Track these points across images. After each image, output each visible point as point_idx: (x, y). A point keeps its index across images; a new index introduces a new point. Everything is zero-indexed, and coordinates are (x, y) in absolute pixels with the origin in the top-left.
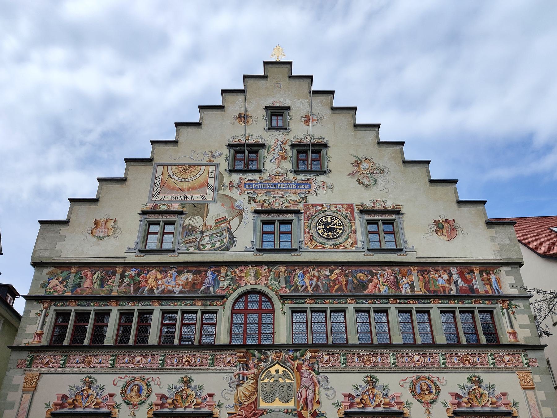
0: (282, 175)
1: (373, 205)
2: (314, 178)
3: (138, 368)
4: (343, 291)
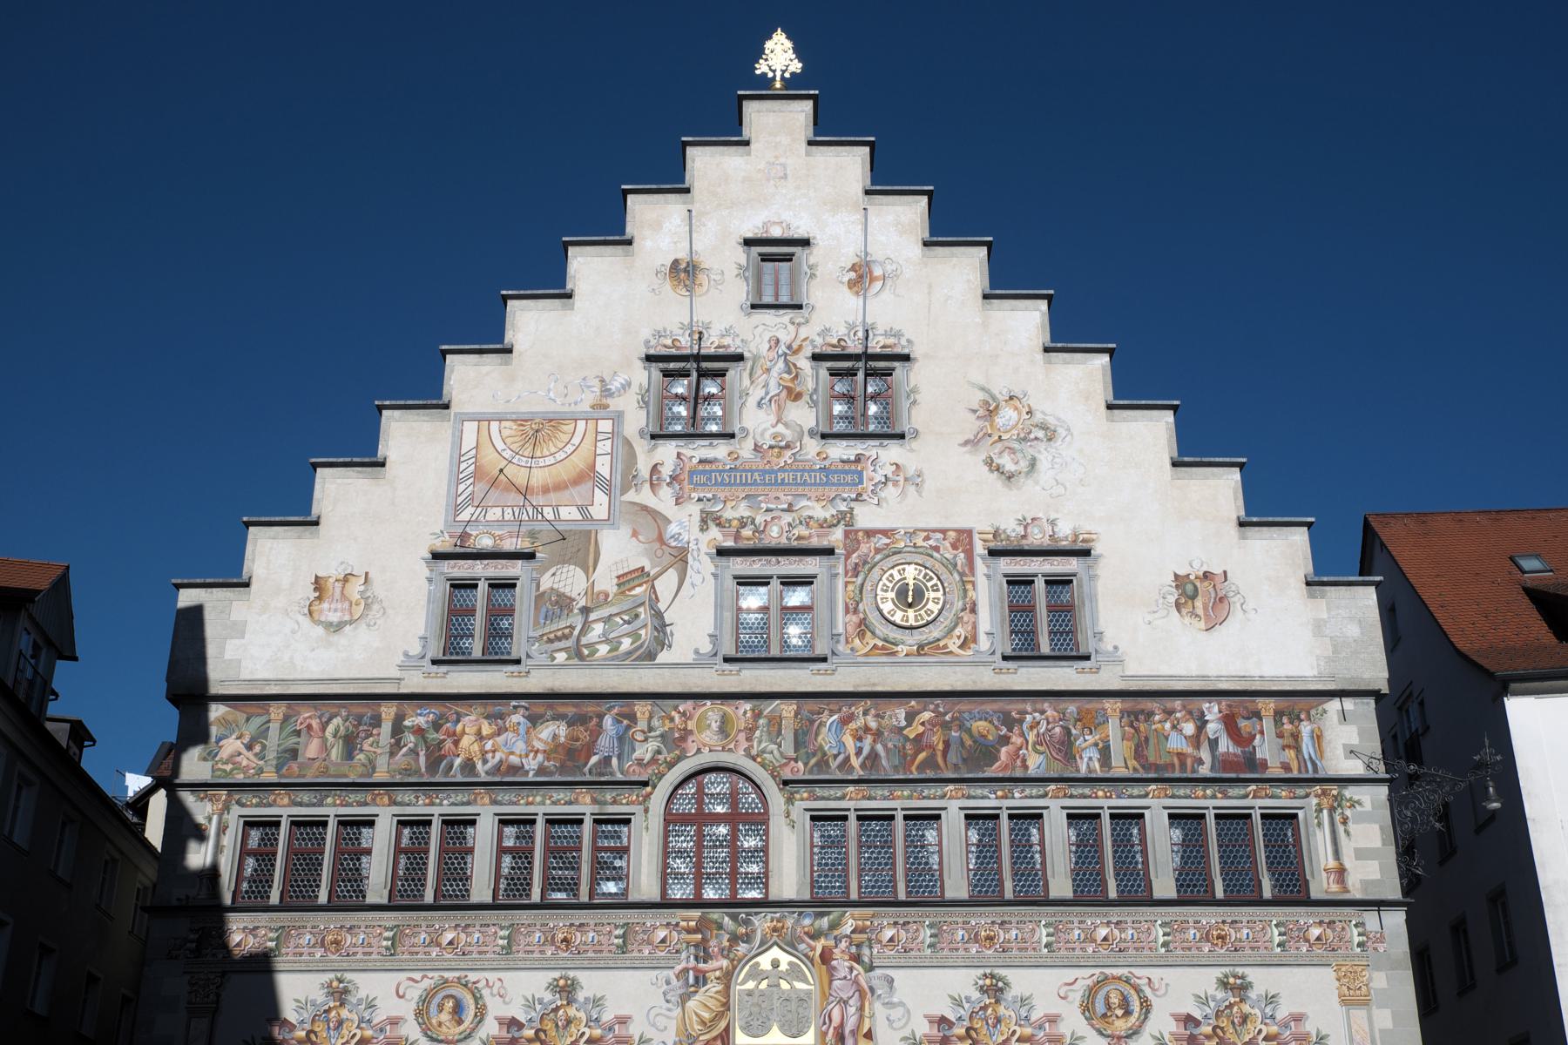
0: (788, 446)
1: (1023, 533)
2: (873, 453)
3: (450, 956)
4: (936, 767)
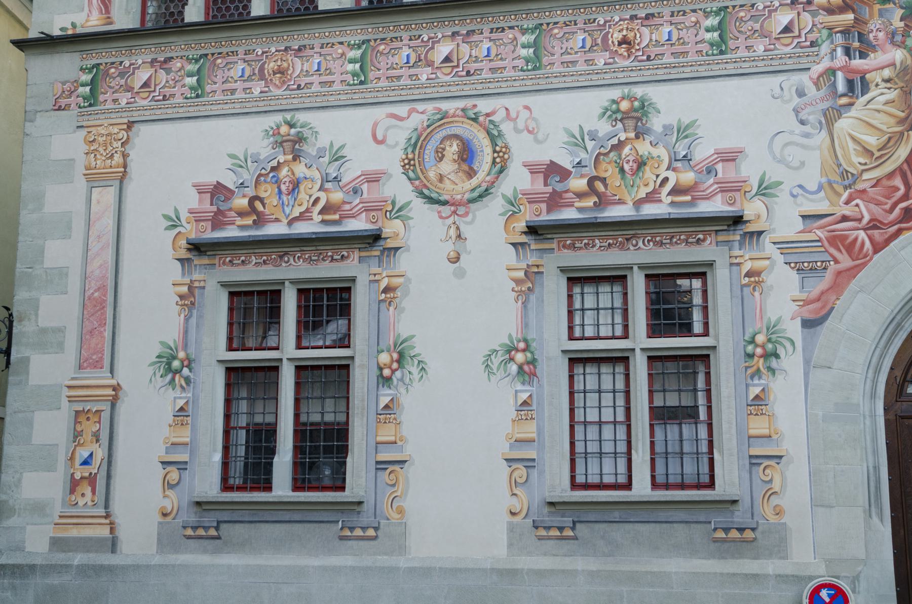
3: (448, 78)
